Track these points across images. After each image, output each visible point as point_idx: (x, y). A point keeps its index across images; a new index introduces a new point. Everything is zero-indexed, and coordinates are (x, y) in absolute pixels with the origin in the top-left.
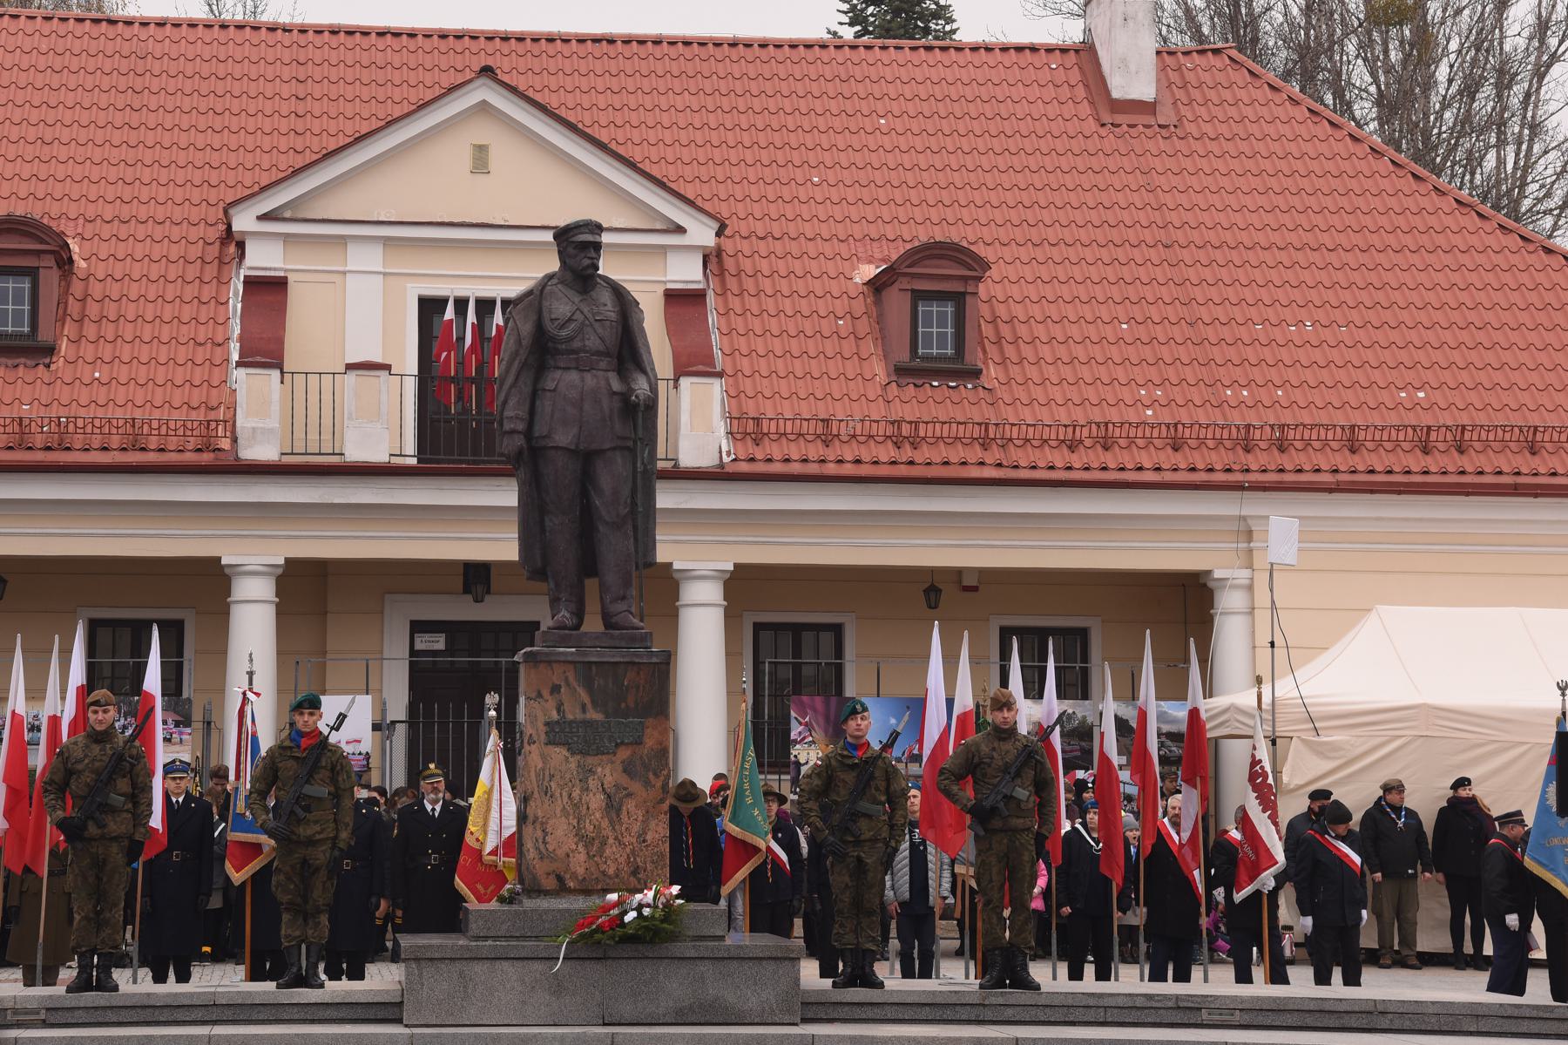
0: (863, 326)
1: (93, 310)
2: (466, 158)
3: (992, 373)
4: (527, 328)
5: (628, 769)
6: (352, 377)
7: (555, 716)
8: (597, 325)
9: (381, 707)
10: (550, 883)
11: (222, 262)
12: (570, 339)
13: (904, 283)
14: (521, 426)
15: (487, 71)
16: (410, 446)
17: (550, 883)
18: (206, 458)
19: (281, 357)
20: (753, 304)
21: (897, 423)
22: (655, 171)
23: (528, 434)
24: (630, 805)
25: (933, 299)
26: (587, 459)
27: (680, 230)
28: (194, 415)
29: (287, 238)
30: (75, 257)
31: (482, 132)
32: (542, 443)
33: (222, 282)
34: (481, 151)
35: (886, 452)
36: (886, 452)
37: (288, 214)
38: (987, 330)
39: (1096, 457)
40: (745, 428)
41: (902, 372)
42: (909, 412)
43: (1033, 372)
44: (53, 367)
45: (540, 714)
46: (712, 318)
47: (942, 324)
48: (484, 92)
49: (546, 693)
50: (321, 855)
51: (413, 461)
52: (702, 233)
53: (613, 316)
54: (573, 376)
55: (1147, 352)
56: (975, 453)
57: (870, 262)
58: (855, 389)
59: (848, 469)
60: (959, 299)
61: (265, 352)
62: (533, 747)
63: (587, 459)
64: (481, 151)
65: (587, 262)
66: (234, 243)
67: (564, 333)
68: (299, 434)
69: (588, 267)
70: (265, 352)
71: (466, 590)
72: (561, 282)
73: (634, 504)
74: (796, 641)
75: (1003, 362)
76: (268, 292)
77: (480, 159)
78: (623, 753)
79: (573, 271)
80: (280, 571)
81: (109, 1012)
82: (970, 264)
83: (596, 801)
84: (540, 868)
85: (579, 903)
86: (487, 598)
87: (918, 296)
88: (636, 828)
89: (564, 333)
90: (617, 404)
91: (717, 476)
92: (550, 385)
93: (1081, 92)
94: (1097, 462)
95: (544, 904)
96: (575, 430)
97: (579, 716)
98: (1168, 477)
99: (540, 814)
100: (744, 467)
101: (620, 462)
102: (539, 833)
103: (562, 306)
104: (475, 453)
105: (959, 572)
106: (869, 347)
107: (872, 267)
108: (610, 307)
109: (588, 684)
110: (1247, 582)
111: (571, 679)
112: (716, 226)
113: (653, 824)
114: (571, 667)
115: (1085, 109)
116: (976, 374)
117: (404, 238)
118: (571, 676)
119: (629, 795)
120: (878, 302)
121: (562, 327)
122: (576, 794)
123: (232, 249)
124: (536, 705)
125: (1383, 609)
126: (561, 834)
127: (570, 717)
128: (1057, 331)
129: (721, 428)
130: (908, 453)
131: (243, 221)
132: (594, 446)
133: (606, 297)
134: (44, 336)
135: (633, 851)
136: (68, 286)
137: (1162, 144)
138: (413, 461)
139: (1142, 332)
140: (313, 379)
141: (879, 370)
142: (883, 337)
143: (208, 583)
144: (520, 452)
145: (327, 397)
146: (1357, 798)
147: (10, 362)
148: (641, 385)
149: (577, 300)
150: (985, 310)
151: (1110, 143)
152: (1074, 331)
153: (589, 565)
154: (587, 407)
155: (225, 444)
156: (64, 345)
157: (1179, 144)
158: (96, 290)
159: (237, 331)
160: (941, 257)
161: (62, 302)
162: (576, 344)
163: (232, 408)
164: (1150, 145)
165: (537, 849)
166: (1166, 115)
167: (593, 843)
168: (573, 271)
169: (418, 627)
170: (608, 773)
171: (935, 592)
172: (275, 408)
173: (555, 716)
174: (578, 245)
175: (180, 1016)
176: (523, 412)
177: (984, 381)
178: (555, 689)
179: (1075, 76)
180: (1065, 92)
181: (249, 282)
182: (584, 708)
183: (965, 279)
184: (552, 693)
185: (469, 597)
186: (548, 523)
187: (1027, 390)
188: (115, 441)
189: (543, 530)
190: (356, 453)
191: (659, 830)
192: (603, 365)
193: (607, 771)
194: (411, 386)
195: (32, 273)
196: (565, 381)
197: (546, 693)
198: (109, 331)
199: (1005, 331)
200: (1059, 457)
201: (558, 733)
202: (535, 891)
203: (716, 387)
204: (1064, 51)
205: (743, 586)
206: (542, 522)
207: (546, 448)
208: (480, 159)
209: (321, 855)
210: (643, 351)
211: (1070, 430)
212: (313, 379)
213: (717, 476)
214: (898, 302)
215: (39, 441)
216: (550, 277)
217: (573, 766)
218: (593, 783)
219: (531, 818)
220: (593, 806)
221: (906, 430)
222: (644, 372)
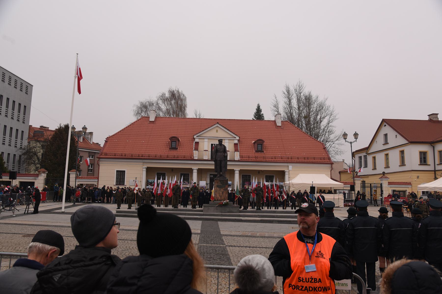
5: (224, 190)
9: (207, 182)
15: (218, 123)
16: (210, 158)
25: (259, 145)
31: (217, 129)
33: (193, 142)
34: (217, 130)
35: (254, 159)
36: (254, 159)
39: (274, 160)
40: (241, 156)
41: (256, 151)
42: (257, 155)
48: (217, 125)
50: (196, 197)
52: (238, 138)
56: (263, 159)
60: (262, 144)
61: (197, 149)
64: (217, 130)
66: (194, 139)
70: (197, 149)
74: (246, 177)
76: (197, 143)
77: (217, 131)
82: (263, 141)
83: (221, 193)
85: (219, 202)
87: (258, 144)
94: (274, 160)
103: (219, 147)
105: (261, 170)
106: (253, 149)
117: (210, 138)
125: (300, 174)
126: (218, 195)
131: (195, 137)
141: (254, 151)
142: (255, 148)
146: (296, 192)
148: (226, 154)
153: (221, 171)
167: (221, 196)
169: (210, 175)
170: (222, 190)
171: (259, 173)
174: (220, 141)
187: (268, 154)
190: (204, 159)
191: (227, 195)
194: (210, 153)
196: (219, 154)
200: (271, 160)
202: (215, 201)
205: (241, 171)
208: (217, 131)
209: (196, 197)
214: (256, 145)
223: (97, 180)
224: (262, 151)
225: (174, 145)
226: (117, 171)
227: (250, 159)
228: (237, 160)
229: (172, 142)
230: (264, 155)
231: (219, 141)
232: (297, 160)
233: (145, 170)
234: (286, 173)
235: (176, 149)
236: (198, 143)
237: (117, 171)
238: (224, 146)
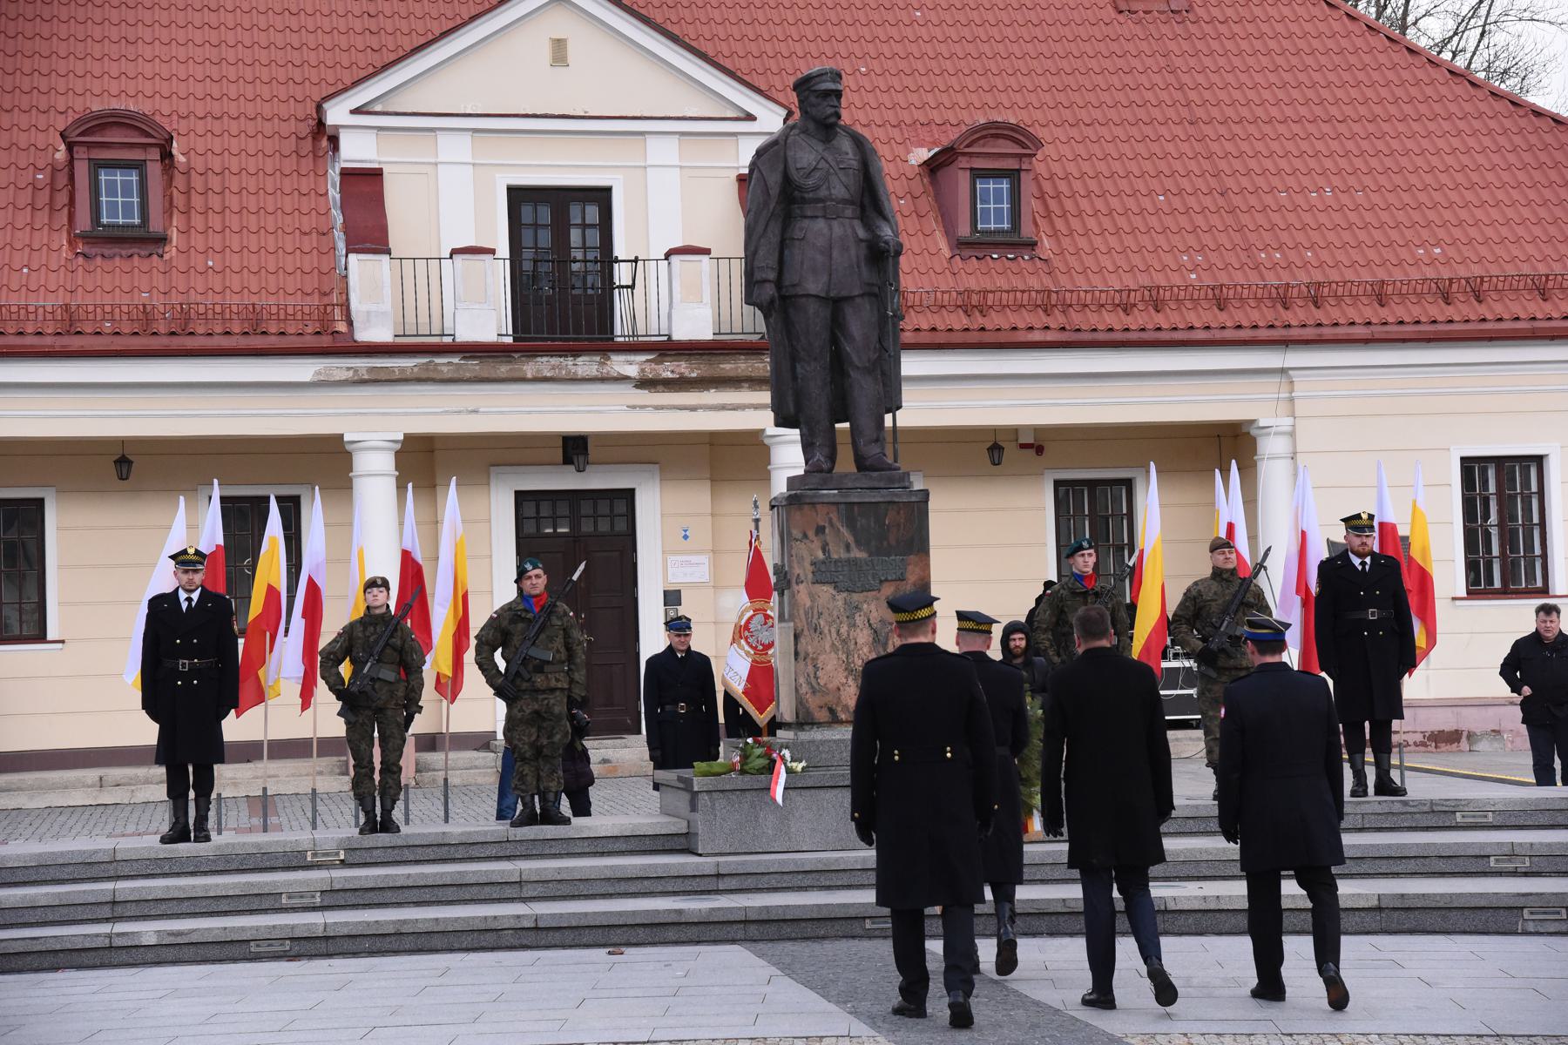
0: (925, 203)
2: (546, 52)
4: (774, 180)
6: (458, 258)
7: (820, 555)
8: (841, 174)
10: (823, 715)
12: (817, 188)
13: (963, 162)
14: (772, 276)
17: (823, 715)
18: (326, 341)
19: (386, 242)
21: (969, 292)
22: (727, 64)
23: (779, 283)
26: (836, 304)
27: (750, 117)
28: (308, 300)
30: (174, 152)
32: (792, 291)
37: (378, 108)
42: (972, 283)
44: (166, 257)
45: (805, 554)
47: (998, 200)
49: (811, 534)
51: (510, 340)
53: (855, 164)
54: (821, 224)
57: (922, 146)
60: (1014, 175)
62: (801, 587)
63: (836, 304)
65: (830, 111)
67: (810, 182)
68: (410, 318)
70: (370, 235)
71: (567, 460)
72: (805, 131)
76: (365, 184)
79: (815, 120)
80: (398, 446)
81: (406, 851)
84: (813, 702)
86: (588, 468)
89: (810, 182)
90: (863, 251)
92: (798, 234)
95: (817, 735)
96: (825, 278)
97: (844, 555)
98: (1218, 335)
99: (810, 649)
102: (810, 669)
103: (806, 155)
104: (577, 330)
105: (1015, 431)
107: (925, 150)
108: (851, 156)
109: (851, 523)
110: (1289, 429)
111: (835, 520)
112: (784, 113)
114: (834, 508)
116: (1032, 245)
118: (834, 516)
120: (934, 181)
121: (808, 175)
122: (844, 629)
123: (324, 143)
124: (802, 546)
127: (835, 556)
130: (980, 321)
131: (336, 114)
132: (844, 293)
133: (846, 145)
134: (156, 226)
136: (171, 179)
137: (1179, 29)
138: (510, 340)
140: (421, 264)
143: (328, 461)
144: (772, 302)
145: (422, 281)
147: (124, 253)
149: (820, 147)
154: (835, 254)
157: (1193, 28)
159: (340, 220)
160: (997, 136)
162: (823, 193)
163: (345, 291)
164: (1164, 29)
165: (809, 683)
168: (815, 120)
172: (388, 291)
175: (475, 852)
176: (773, 261)
177: (1038, 252)
178: (820, 530)
181: (346, 173)
183: (1020, 156)
184: (817, 534)
185: (572, 468)
186: (799, 369)
189: (795, 378)
193: (873, 607)
195: (139, 166)
196: (816, 230)
197: (811, 534)
201: (824, 573)
206: (793, 369)
207: (796, 296)
210: (883, 198)
211: (1124, 295)
212: (421, 264)
217: (840, 603)
218: (859, 620)
219: (802, 655)
220: (861, 641)
221: (975, 299)
222: (886, 219)
224: (1015, 243)
225: (119, 199)
230: (1048, 282)
231: (796, 87)
232: (1371, 312)
234: (1271, 448)
235: (145, 240)
236: (375, 175)
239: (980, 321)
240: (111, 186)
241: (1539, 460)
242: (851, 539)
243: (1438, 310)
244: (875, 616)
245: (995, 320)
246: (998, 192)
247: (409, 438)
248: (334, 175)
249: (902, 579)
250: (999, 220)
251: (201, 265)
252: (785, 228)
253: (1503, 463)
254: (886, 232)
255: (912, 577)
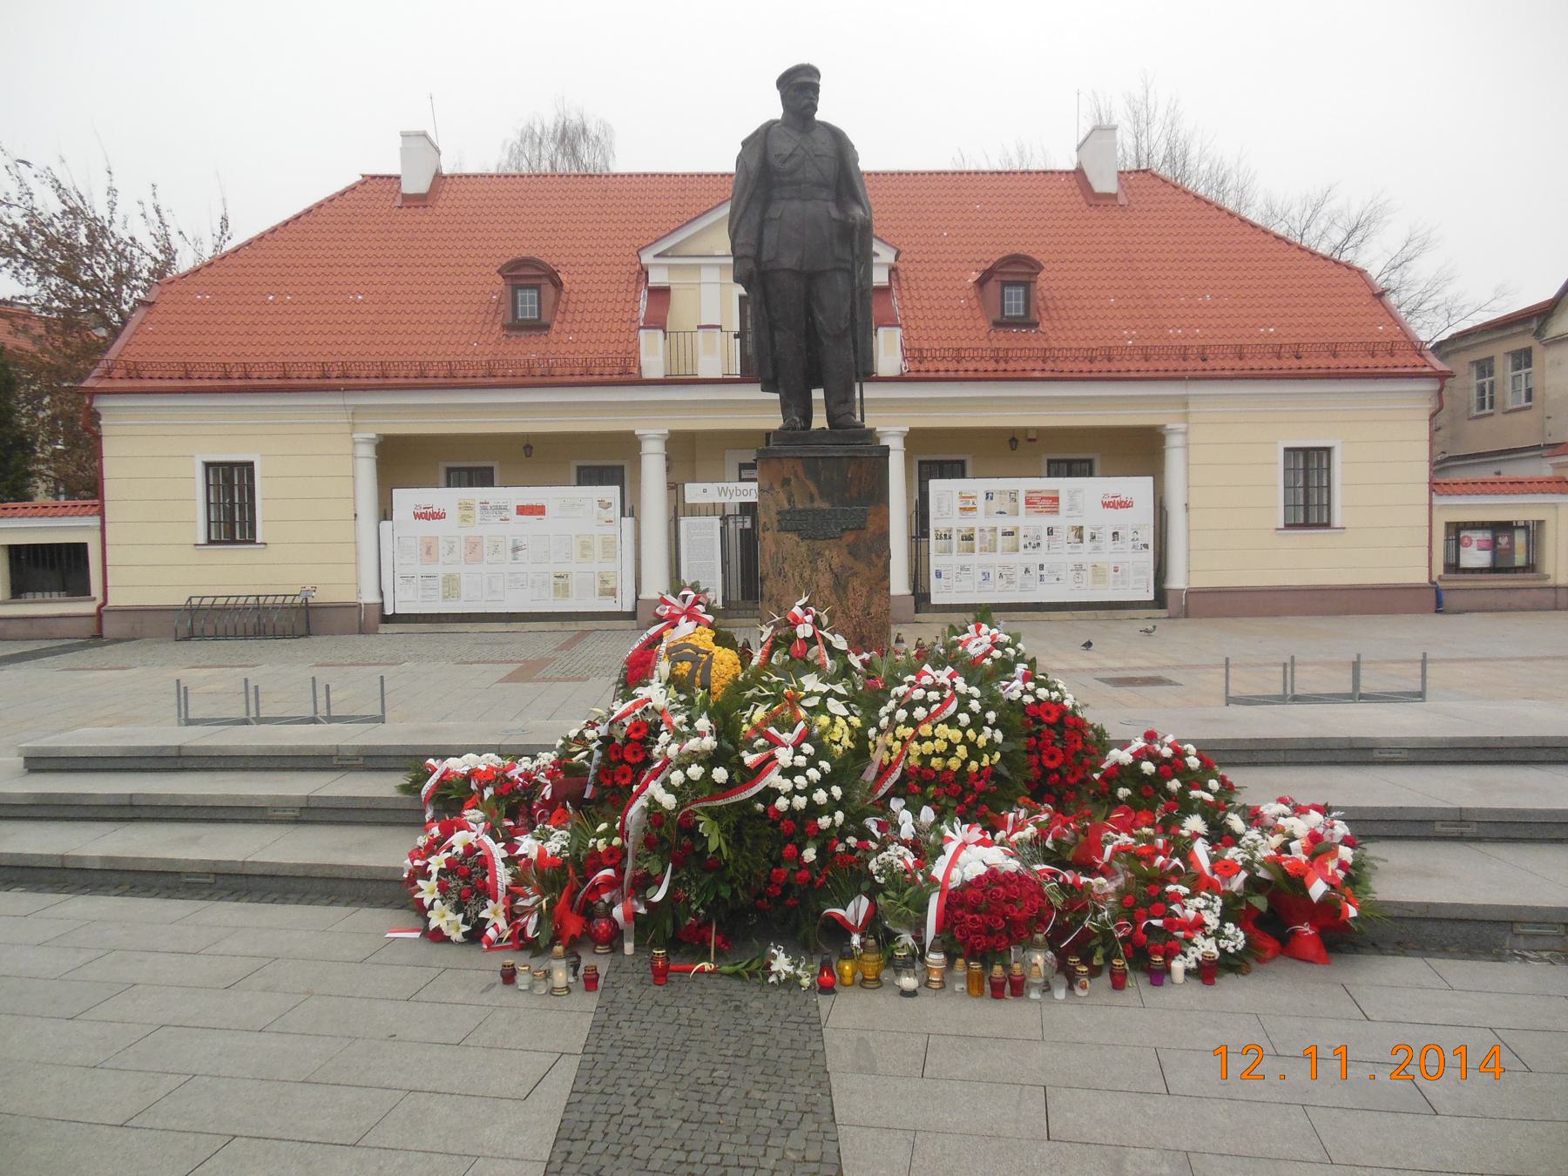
0: (974, 303)
1: (571, 307)
3: (1045, 326)
4: (754, 163)
5: (853, 552)
7: (786, 506)
11: (638, 282)
12: (792, 172)
13: (997, 277)
20: (915, 294)
24: (856, 582)
29: (670, 266)
33: (637, 292)
35: (991, 366)
36: (991, 366)
38: (1041, 304)
40: (909, 353)
42: (1003, 344)
43: (1066, 323)
46: (895, 302)
55: (1126, 313)
56: (1040, 365)
58: (973, 334)
59: (971, 374)
60: (1027, 285)
61: (657, 321)
62: (768, 534)
65: (806, 101)
66: (644, 272)
67: (787, 166)
69: (806, 107)
70: (657, 321)
73: (853, 315)
75: (1050, 319)
76: (661, 294)
78: (849, 538)
88: (863, 601)
91: (900, 379)
93: (1077, 191)
97: (808, 506)
100: (913, 375)
101: (840, 279)
105: (1026, 430)
113: (876, 600)
115: (1081, 198)
116: (1036, 325)
119: (855, 574)
121: (784, 162)
122: (806, 574)
127: (800, 506)
128: (1077, 303)
129: (899, 356)
131: (647, 258)
135: (859, 623)
139: (1121, 302)
141: (984, 324)
150: (1039, 294)
151: (1095, 213)
152: (1086, 303)
155: (635, 370)
156: (555, 326)
158: (574, 298)
161: (556, 304)
163: (638, 352)
166: (1122, 200)
170: (834, 555)
173: (786, 506)
179: (1074, 184)
180: (1070, 191)
182: (812, 499)
183: (1029, 274)
186: (777, 337)
188: (577, 370)
189: (773, 346)
190: (702, 375)
192: (824, 195)
195: (538, 287)
196: (788, 209)
198: (578, 317)
199: (1050, 304)
200: (1085, 366)
203: (898, 332)
204: (1068, 172)
205: (915, 439)
213: (900, 379)
215: (538, 372)
216: (774, 122)
218: (821, 565)
220: (822, 584)
222: (860, 203)
223: (95, 521)
224: (1027, 323)
225: (528, 304)
226: (208, 465)
227: (964, 365)
228: (895, 372)
229: (515, 288)
233: (367, 453)
234: (1174, 442)
235: (539, 326)
237: (208, 465)
238: (837, 137)
239: (1002, 366)
240: (524, 299)
241: (1328, 450)
242: (813, 489)
243: (1275, 363)
244: (836, 561)
245: (1012, 366)
246: (1017, 295)
247: (672, 433)
248: (644, 293)
249: (861, 528)
250: (1017, 309)
251: (568, 342)
252: (764, 211)
253: (1307, 451)
254: (858, 212)
255: (871, 528)
